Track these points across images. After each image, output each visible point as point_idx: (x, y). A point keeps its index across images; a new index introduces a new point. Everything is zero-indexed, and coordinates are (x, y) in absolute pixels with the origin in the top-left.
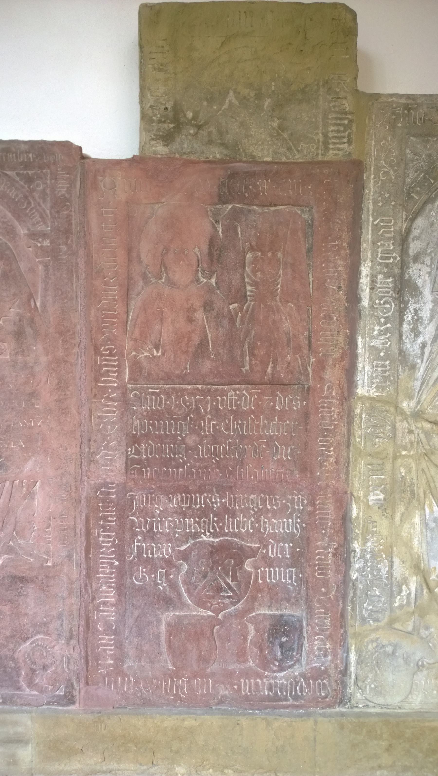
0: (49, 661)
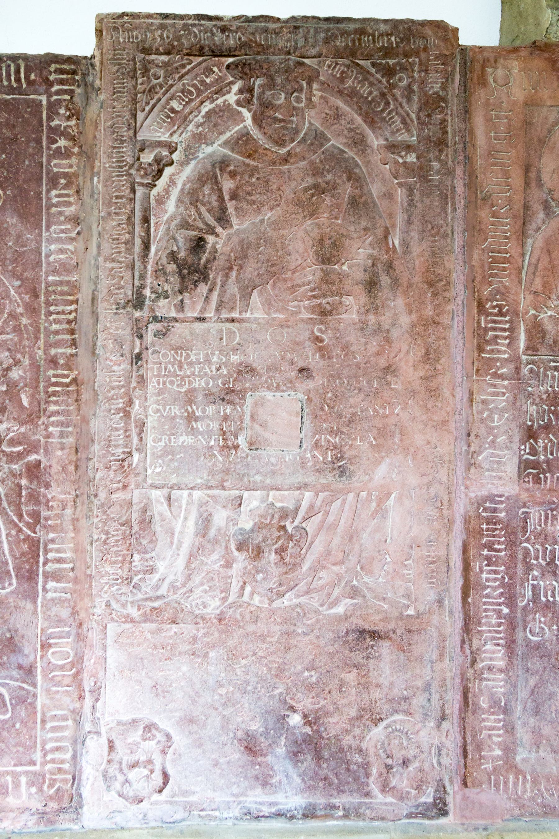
0: (410, 754)
